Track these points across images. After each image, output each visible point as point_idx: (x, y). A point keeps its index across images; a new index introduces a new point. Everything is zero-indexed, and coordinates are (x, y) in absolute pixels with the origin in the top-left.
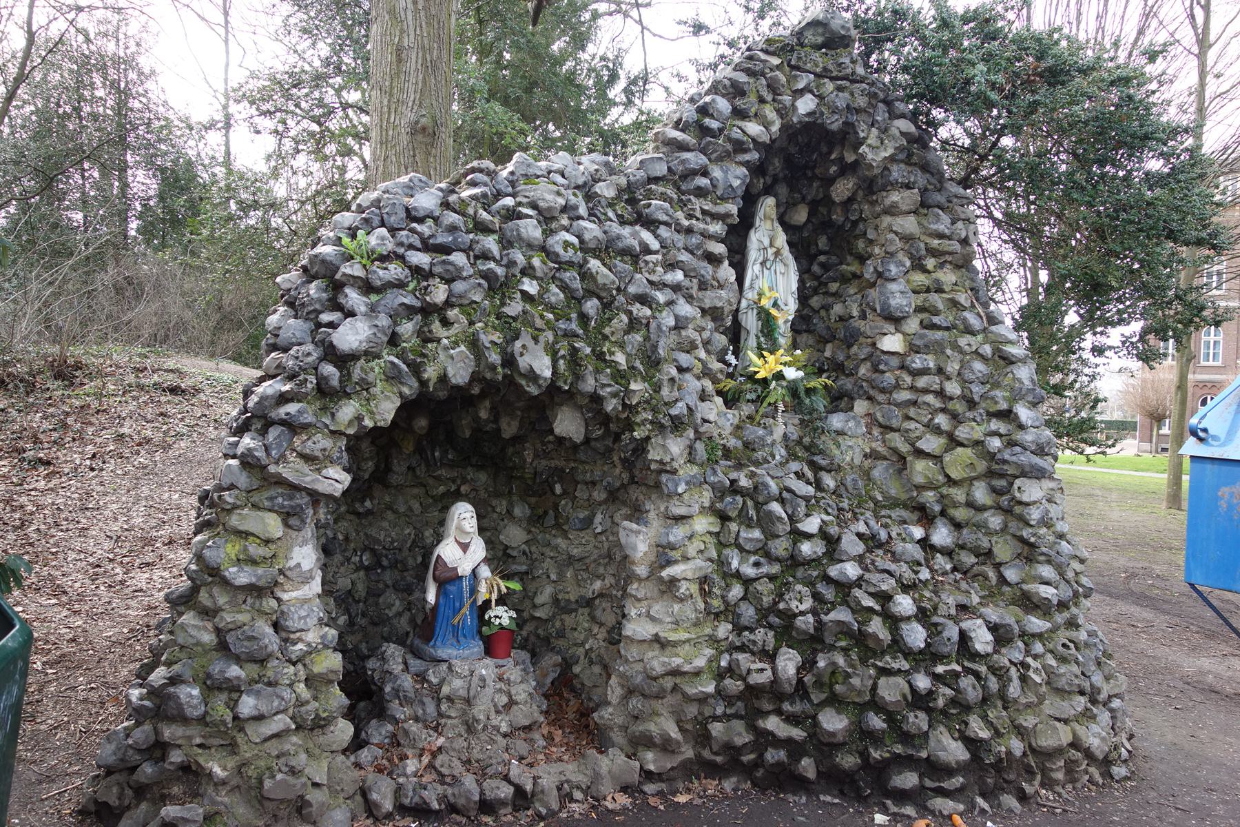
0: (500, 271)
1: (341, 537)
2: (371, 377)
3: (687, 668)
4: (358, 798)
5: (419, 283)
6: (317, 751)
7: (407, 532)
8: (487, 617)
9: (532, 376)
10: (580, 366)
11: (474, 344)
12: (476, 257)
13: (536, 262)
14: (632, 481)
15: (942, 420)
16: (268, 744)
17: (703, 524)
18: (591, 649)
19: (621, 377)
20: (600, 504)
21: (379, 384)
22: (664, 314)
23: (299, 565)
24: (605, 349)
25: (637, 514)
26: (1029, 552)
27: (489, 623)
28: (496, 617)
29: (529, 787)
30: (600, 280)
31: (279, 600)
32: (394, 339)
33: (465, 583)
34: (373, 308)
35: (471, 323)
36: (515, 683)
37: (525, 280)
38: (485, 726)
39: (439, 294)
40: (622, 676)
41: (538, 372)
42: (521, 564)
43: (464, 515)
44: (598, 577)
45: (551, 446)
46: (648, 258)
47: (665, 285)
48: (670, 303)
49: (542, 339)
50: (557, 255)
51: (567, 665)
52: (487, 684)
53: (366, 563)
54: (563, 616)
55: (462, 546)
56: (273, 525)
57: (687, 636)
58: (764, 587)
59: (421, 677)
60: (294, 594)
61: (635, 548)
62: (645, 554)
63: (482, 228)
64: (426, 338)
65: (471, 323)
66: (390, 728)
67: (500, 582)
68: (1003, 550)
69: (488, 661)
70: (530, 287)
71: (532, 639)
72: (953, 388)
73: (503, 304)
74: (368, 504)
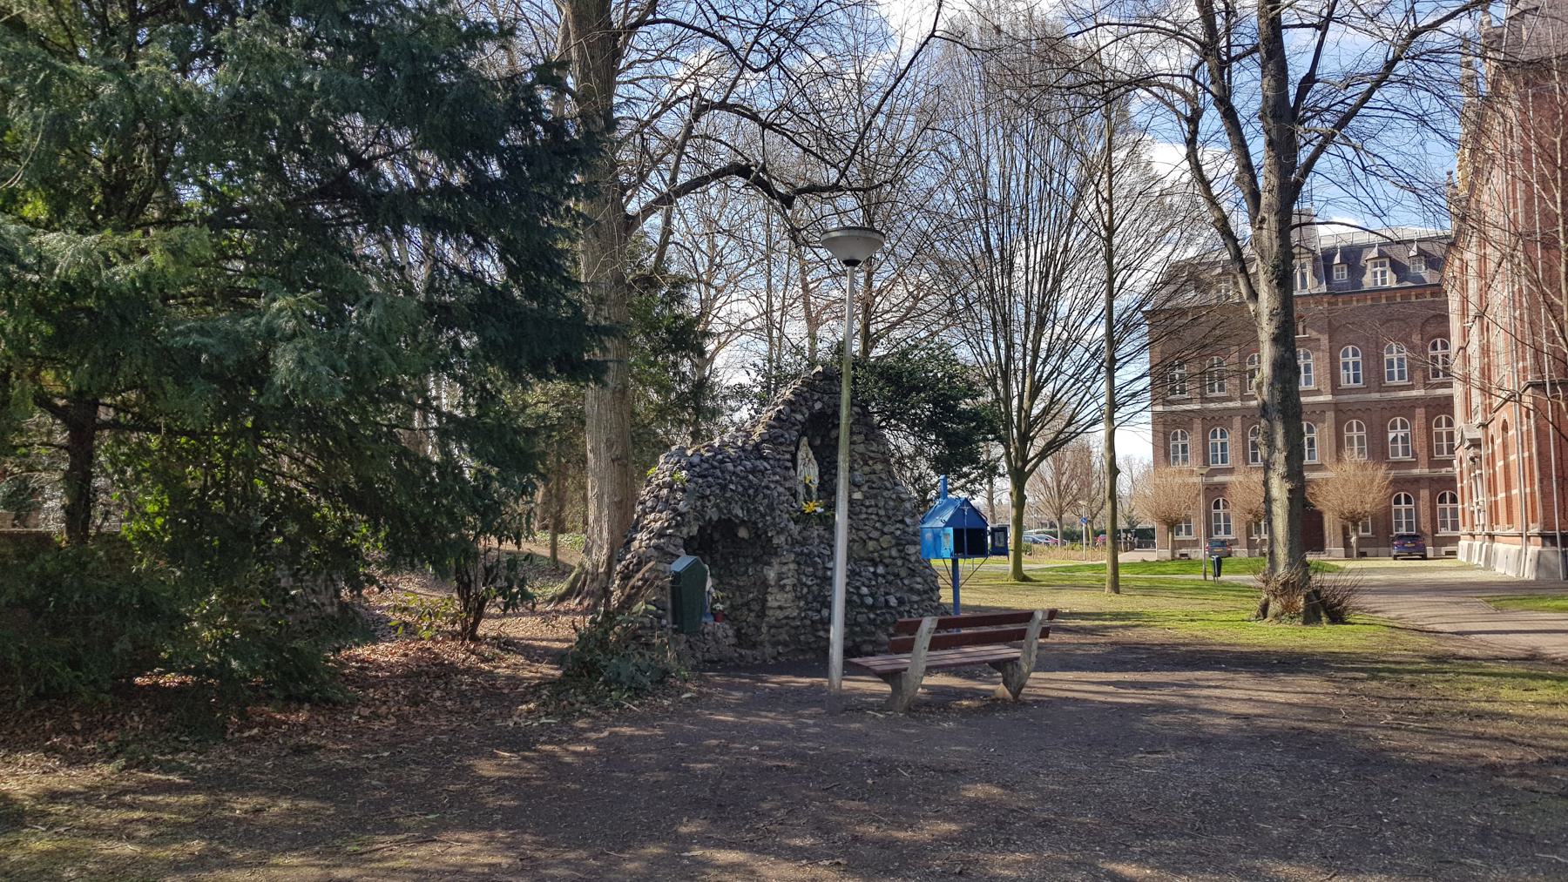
17: (792, 566)
19: (763, 516)
25: (769, 564)
26: (913, 573)
58: (815, 588)
64: (703, 506)
68: (903, 573)
72: (882, 512)
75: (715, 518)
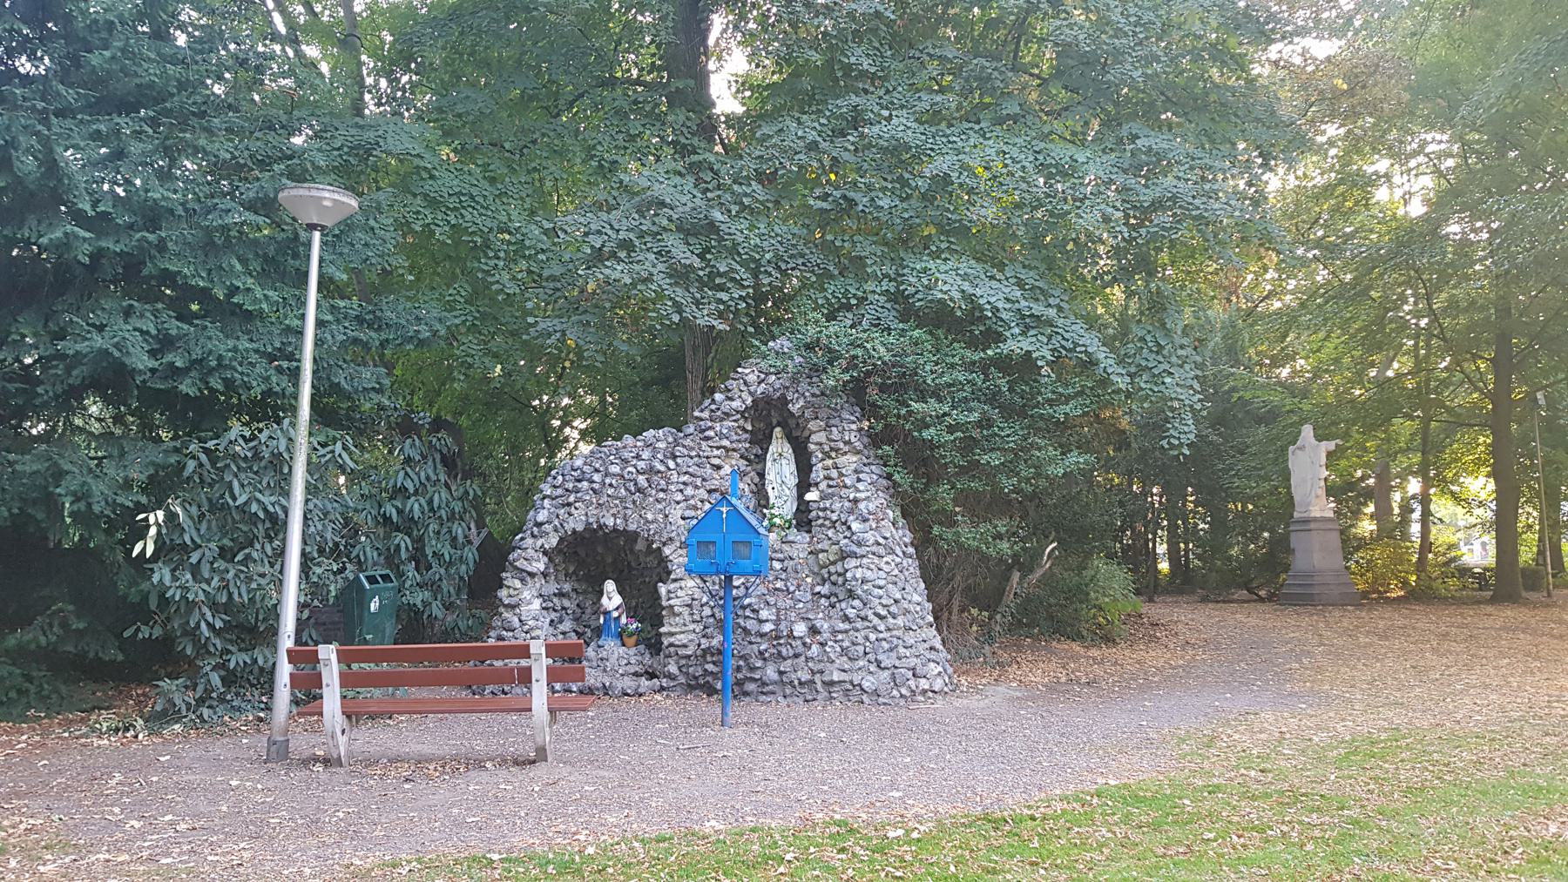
15: (830, 533)
55: (612, 599)
56: (518, 584)
63: (597, 471)
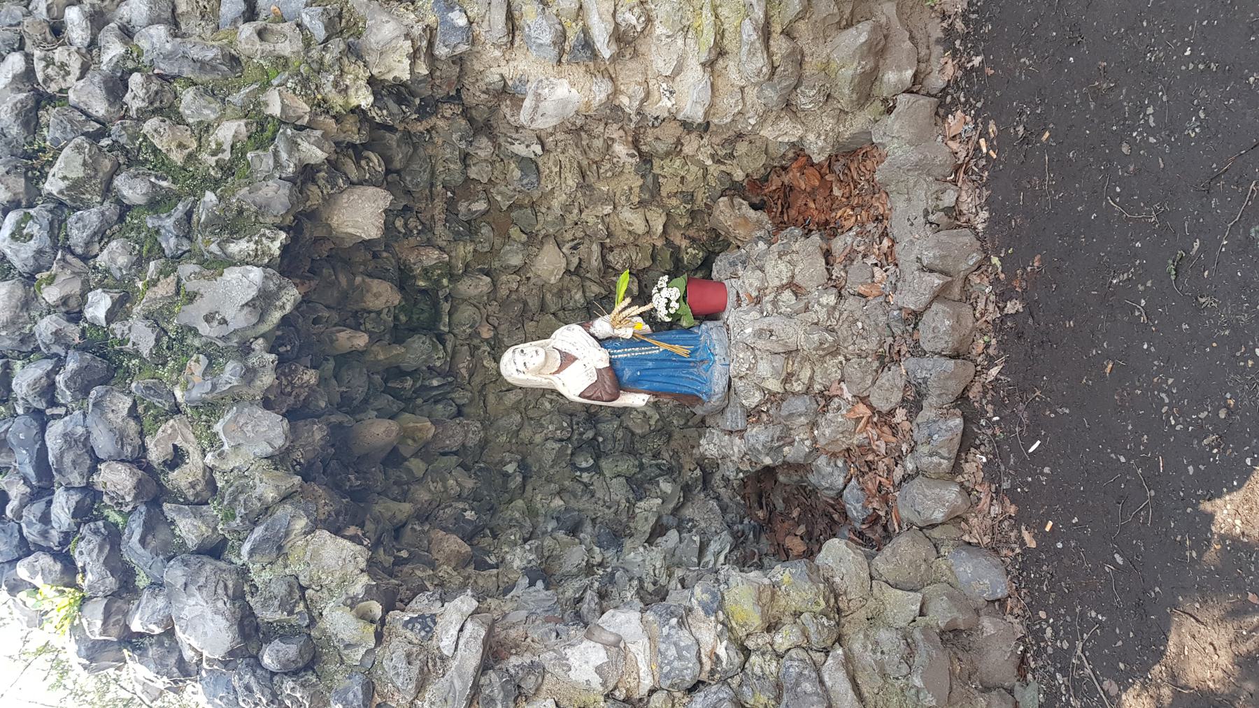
0: (71, 365)
1: (558, 502)
2: (280, 589)
3: (759, 14)
4: (936, 533)
5: (106, 506)
6: (871, 603)
7: (548, 405)
8: (668, 320)
9: (262, 302)
10: (241, 212)
11: (210, 408)
12: (53, 403)
13: (51, 294)
14: (457, 98)
16: (865, 689)
18: (712, 156)
19: (262, 131)
20: (497, 146)
21: (294, 568)
22: (144, 44)
23: (599, 670)
24: (212, 161)
27: (676, 317)
28: (668, 307)
29: (936, 280)
30: (78, 172)
31: (652, 691)
32: (214, 550)
33: (621, 354)
34: (157, 586)
35: (176, 410)
36: (764, 280)
37: (89, 313)
38: (830, 330)
39: (117, 479)
40: (762, 120)
41: (253, 293)
42: (590, 252)
43: (522, 364)
44: (609, 147)
45: (412, 223)
46: (40, 76)
47: (93, 43)
48: (127, 33)
49: (190, 286)
50: (40, 252)
51: (733, 189)
52: (770, 333)
53: (591, 462)
54: (664, 194)
55: (563, 363)
57: (707, 13)
59: (752, 414)
60: (643, 668)
61: (564, 103)
62: (573, 85)
65: (176, 410)
66: (822, 461)
67: (618, 308)
69: (731, 315)
70: (99, 306)
71: (691, 232)
73: (137, 354)
74: (510, 468)
75: (270, 430)
